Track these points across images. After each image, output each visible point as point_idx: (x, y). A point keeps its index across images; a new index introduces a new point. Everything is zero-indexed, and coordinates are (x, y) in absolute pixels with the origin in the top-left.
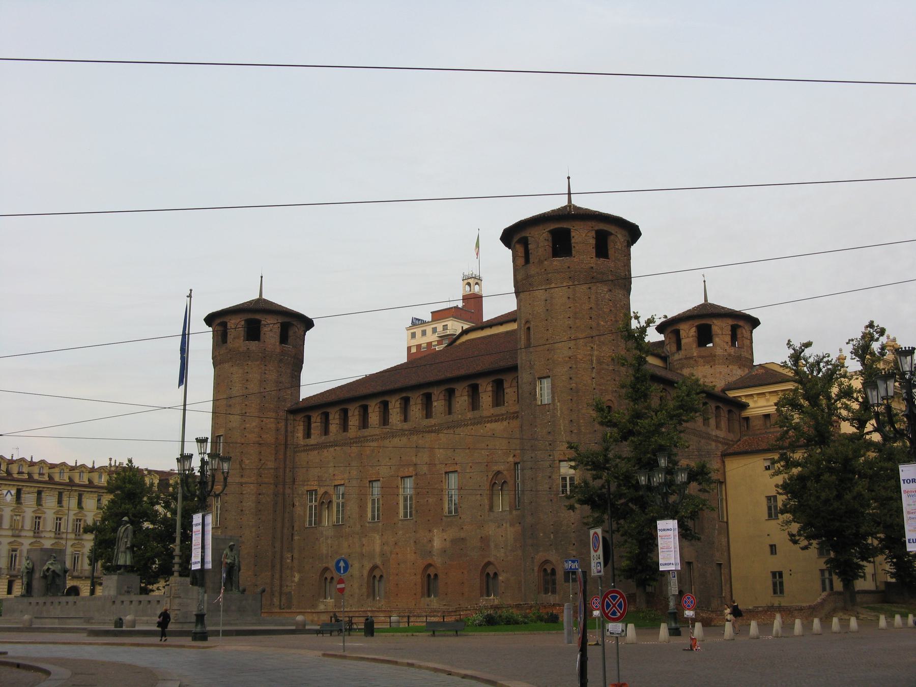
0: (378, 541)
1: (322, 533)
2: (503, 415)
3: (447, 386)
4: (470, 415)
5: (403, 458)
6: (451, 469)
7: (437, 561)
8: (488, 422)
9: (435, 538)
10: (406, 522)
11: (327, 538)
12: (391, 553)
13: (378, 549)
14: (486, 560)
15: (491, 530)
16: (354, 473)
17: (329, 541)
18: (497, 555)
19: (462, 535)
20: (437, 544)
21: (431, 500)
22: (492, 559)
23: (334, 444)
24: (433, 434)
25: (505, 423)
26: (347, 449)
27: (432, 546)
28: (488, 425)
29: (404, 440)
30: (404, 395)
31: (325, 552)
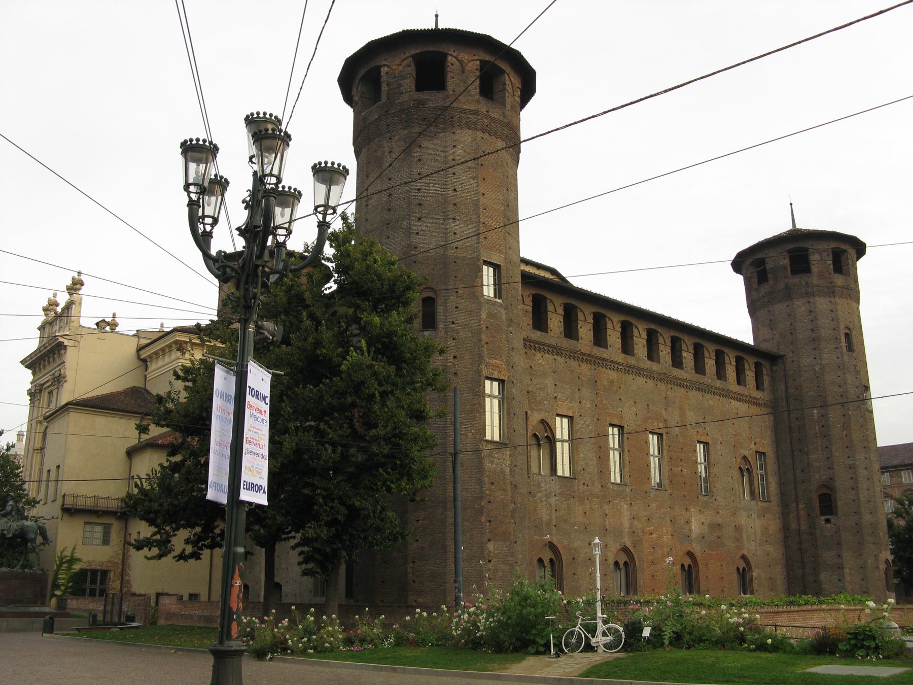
0: (626, 514)
1: (539, 485)
2: (745, 396)
3: (697, 340)
4: (718, 383)
5: (651, 407)
6: (703, 439)
7: (697, 549)
8: (734, 399)
9: (693, 520)
10: (659, 493)
11: (548, 495)
12: (643, 532)
13: (626, 524)
14: (741, 553)
15: (743, 519)
16: (587, 405)
17: (553, 500)
18: (751, 548)
19: (719, 520)
20: (695, 527)
21: (685, 471)
22: (745, 553)
23: (555, 350)
24: (682, 390)
25: (746, 405)
26: (573, 363)
27: (690, 530)
28: (733, 401)
29: (651, 383)
30: (653, 327)
31: (545, 517)
